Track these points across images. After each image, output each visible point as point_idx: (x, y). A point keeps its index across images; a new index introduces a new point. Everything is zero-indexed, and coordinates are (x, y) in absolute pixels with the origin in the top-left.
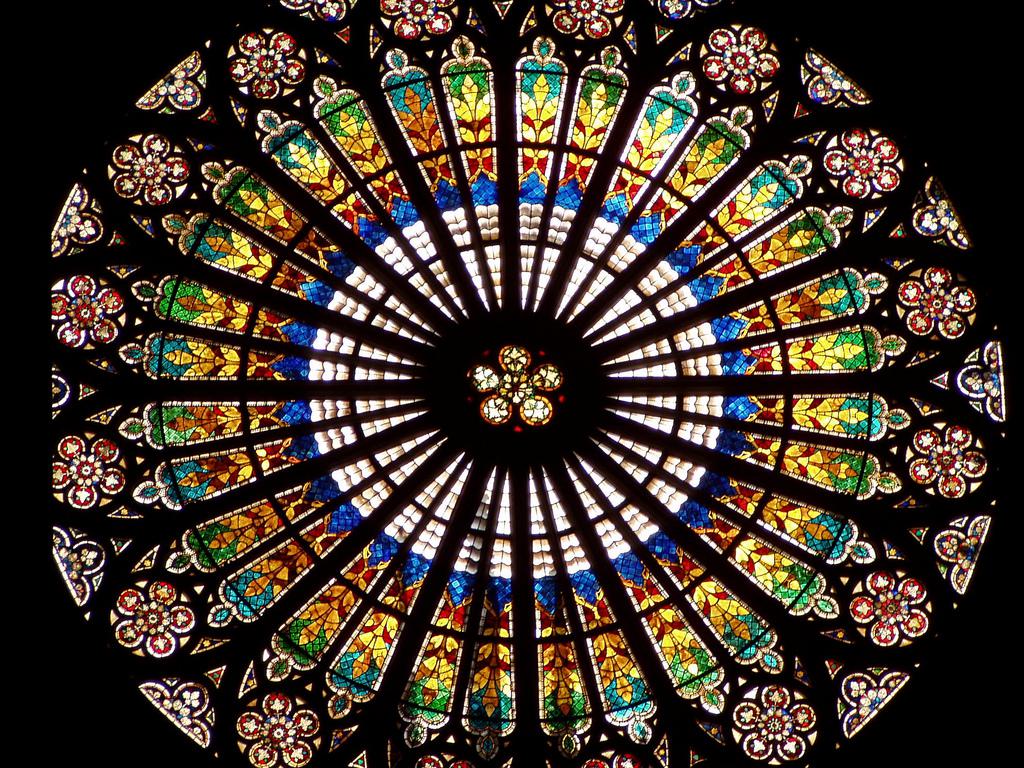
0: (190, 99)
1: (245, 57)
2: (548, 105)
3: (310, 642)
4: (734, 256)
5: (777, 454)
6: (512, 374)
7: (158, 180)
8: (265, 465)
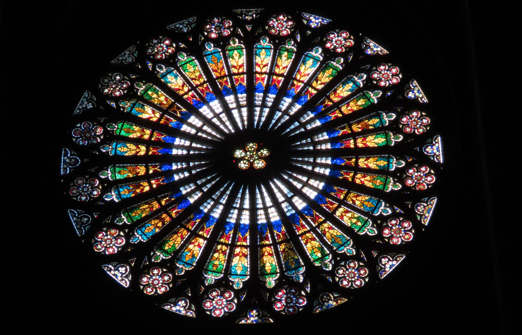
0: (130, 61)
1: (152, 46)
2: (266, 60)
3: (169, 248)
5: (352, 177)
6: (250, 152)
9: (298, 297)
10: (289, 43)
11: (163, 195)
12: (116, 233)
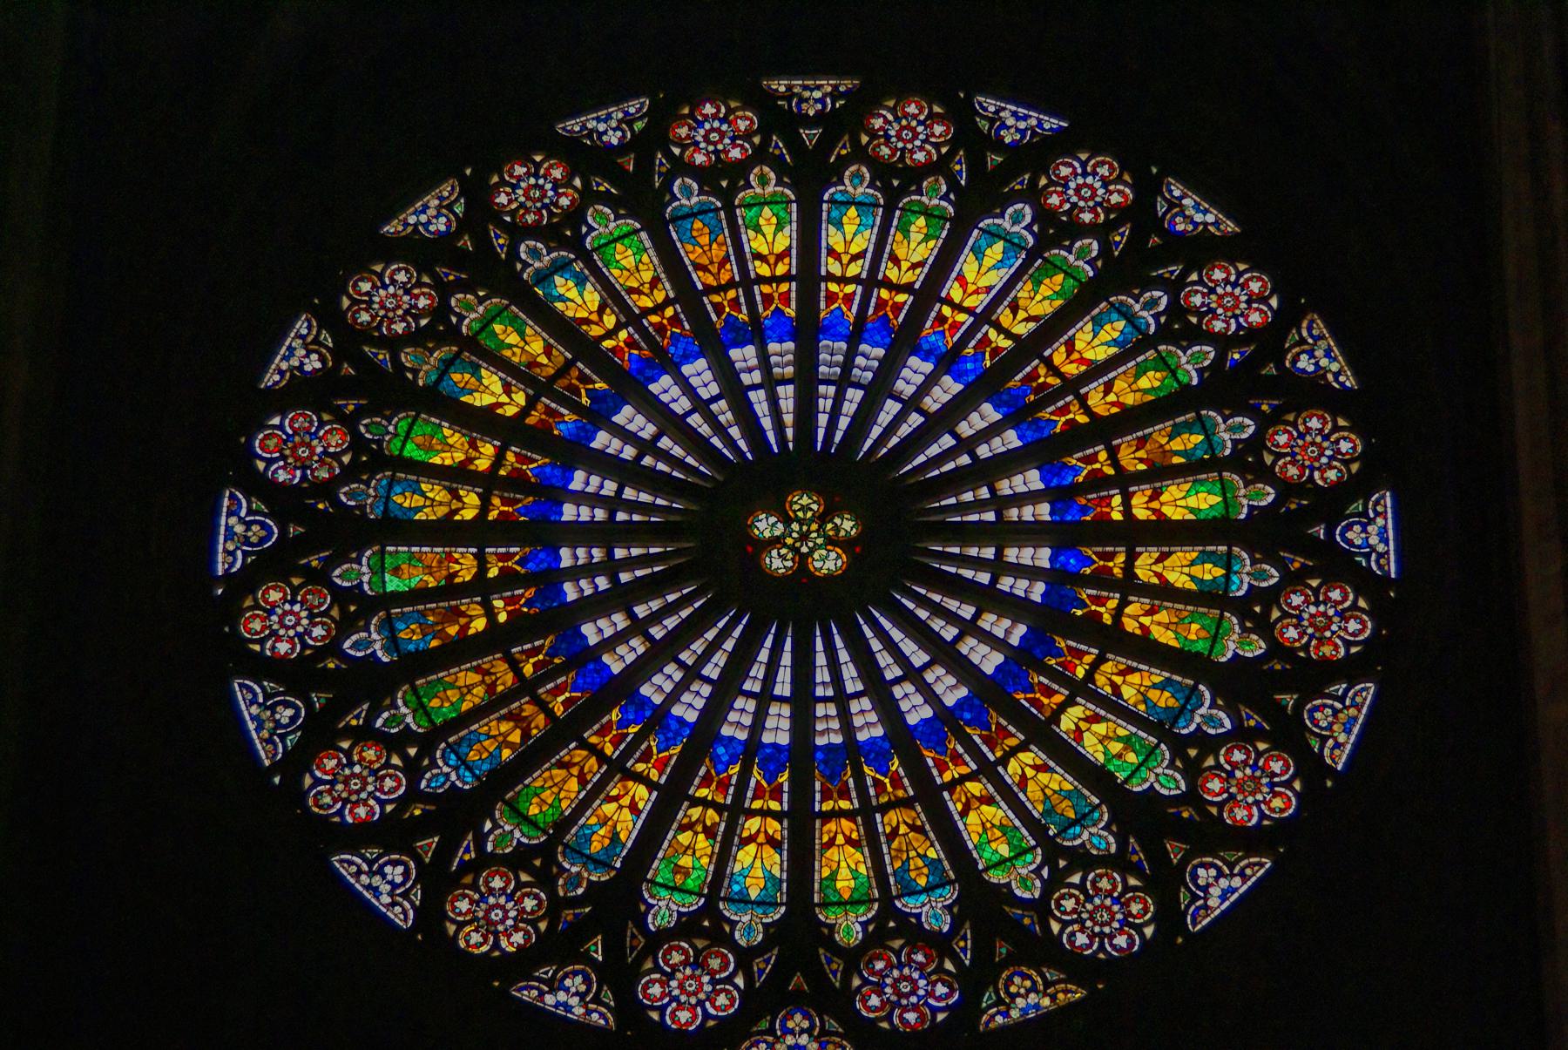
0: (443, 228)
2: (858, 238)
6: (801, 522)
7: (400, 312)
9: (934, 978)
10: (934, 190)
11: (528, 646)
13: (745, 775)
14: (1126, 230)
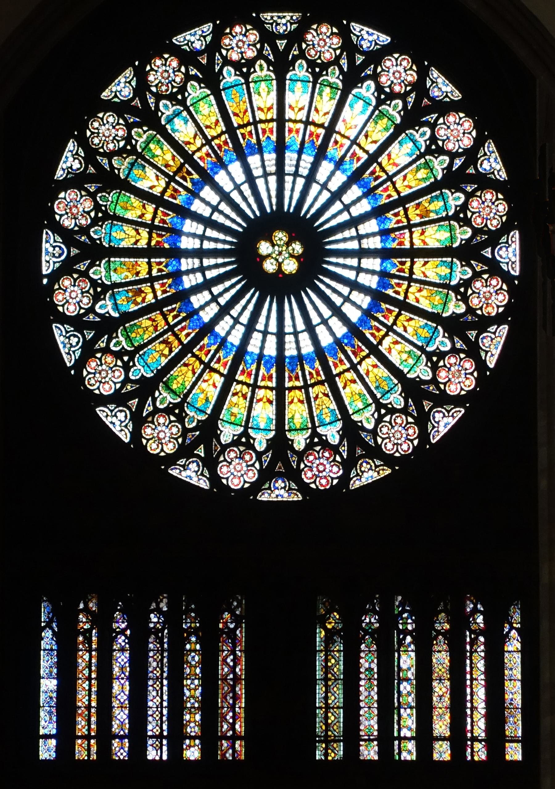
4: (389, 183)
6: (279, 246)
7: (111, 138)
8: (159, 293)
9: (332, 464)
11: (170, 308)
12: (112, 361)
13: (258, 369)
14: (413, 95)
